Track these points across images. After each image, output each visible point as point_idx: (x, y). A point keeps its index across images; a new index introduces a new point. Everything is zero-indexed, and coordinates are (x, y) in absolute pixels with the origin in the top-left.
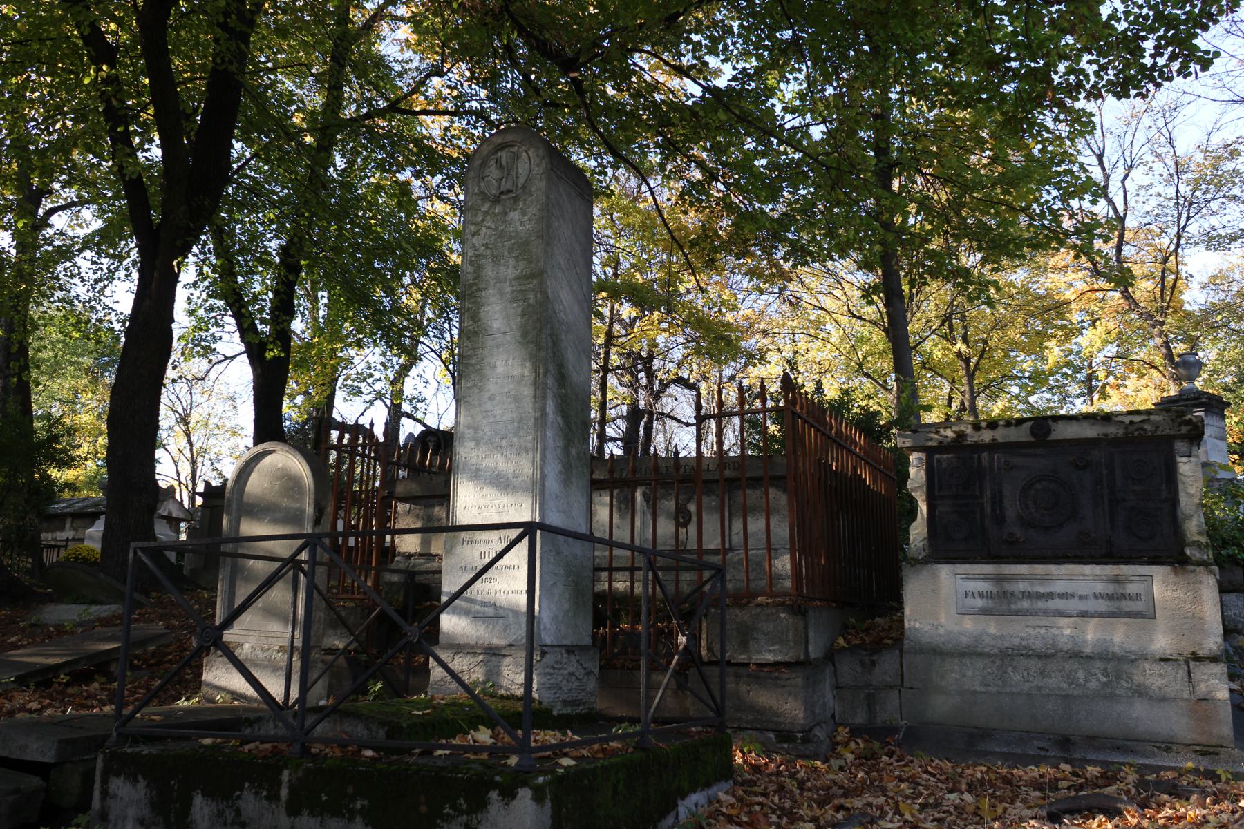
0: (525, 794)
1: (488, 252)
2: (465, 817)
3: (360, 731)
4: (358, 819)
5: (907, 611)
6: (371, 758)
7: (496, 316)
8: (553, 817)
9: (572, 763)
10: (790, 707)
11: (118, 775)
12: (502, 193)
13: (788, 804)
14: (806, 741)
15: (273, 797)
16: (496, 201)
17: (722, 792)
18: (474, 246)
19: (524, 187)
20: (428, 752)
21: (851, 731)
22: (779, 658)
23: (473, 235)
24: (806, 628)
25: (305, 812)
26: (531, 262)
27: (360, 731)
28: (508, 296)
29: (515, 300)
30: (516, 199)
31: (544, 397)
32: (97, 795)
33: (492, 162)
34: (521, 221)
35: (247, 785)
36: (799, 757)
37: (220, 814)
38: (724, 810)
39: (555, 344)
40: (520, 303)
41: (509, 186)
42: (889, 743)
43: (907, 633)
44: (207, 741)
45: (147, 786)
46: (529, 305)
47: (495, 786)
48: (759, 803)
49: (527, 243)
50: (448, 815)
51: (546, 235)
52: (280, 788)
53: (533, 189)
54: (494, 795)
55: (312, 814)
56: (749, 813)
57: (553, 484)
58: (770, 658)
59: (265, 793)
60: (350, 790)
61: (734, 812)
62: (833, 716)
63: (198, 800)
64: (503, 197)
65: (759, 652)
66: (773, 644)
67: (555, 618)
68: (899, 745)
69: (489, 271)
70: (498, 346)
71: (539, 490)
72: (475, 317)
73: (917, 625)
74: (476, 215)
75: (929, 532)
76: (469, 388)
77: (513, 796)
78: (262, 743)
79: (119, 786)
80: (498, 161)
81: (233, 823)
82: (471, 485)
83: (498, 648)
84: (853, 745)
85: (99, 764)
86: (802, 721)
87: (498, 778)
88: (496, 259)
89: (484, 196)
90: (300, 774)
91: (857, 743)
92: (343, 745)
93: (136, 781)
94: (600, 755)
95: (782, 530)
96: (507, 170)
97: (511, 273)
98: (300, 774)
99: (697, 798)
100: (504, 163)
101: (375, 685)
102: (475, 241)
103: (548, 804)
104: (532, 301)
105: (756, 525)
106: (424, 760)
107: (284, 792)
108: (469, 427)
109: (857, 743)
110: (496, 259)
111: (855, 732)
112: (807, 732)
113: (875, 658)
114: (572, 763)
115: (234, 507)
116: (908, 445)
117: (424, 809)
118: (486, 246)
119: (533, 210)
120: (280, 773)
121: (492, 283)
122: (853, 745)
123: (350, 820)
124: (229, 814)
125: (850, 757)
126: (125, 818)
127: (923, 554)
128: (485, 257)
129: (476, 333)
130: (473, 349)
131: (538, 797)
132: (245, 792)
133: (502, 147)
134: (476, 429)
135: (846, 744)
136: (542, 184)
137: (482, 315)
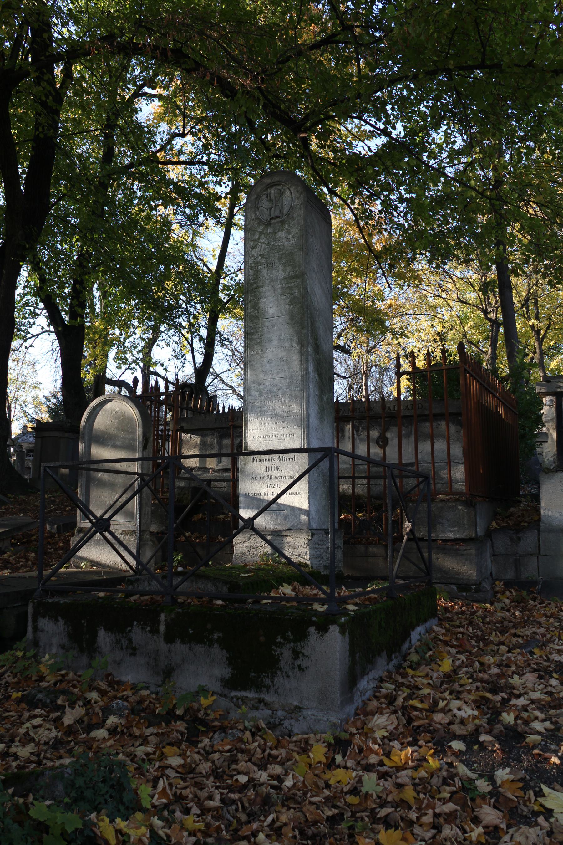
0: (334, 630)
1: (264, 261)
2: (292, 644)
3: (210, 587)
4: (216, 645)
5: (543, 504)
6: (221, 605)
7: (271, 305)
8: (350, 644)
9: (355, 608)
10: (467, 570)
11: (44, 617)
12: (272, 218)
13: (480, 633)
14: (478, 591)
15: (155, 631)
16: (268, 224)
17: (433, 624)
18: (253, 256)
19: (288, 214)
20: (257, 602)
21: (504, 584)
22: (458, 536)
23: (252, 249)
24: (475, 516)
25: (178, 641)
26: (295, 267)
27: (210, 587)
28: (279, 291)
29: (285, 294)
30: (283, 223)
31: (307, 361)
32: (30, 629)
33: (264, 197)
34: (287, 238)
35: (135, 623)
36: (474, 601)
37: (118, 642)
38: (441, 637)
39: (313, 324)
40: (288, 296)
41: (277, 213)
42: (532, 592)
43: (543, 519)
44: (102, 594)
45: (65, 624)
46: (294, 298)
47: (313, 624)
48: (461, 633)
49: (292, 254)
50: (280, 643)
51: (305, 248)
52: (159, 625)
53: (295, 215)
54: (312, 630)
55: (183, 642)
56: (457, 639)
57: (314, 421)
58: (451, 536)
59: (148, 629)
60: (209, 626)
61: (447, 638)
62: (491, 574)
63: (102, 633)
64: (273, 221)
65: (443, 532)
66: (453, 527)
67: (318, 511)
68: (539, 593)
69: (264, 273)
70: (273, 326)
71: (304, 423)
72: (256, 306)
73: (550, 513)
74: (254, 235)
75: (558, 450)
76: (253, 355)
77: (326, 630)
78: (141, 595)
79: (45, 624)
80: (268, 196)
81: (127, 648)
82: (257, 422)
83: (280, 531)
84: (508, 593)
85: (30, 609)
86: (475, 578)
87: (314, 619)
88: (269, 265)
89: (260, 222)
90: (173, 616)
91: (511, 592)
92: (199, 597)
93: (57, 620)
94: (367, 603)
95: (457, 451)
96: (275, 202)
97: (281, 274)
98: (173, 616)
99: (420, 629)
100: (273, 197)
101: (178, 555)
102: (253, 252)
103: (347, 635)
104: (296, 294)
105: (440, 445)
106: (257, 607)
107: (162, 628)
108: (254, 382)
109: (511, 592)
110: (269, 265)
111: (508, 585)
112: (478, 585)
113: (520, 535)
114: (355, 608)
115: (86, 438)
116: (543, 391)
117: (262, 639)
118: (262, 256)
119: (295, 230)
120: (158, 615)
121: (267, 282)
122: (508, 593)
123: (210, 646)
124: (124, 642)
125: (507, 601)
126: (51, 645)
127: (554, 465)
128: (261, 264)
129: (257, 317)
130: (255, 328)
131: (342, 632)
132: (135, 628)
133: (270, 186)
134: (259, 384)
135: (503, 593)
136: (301, 212)
137: (261, 304)
